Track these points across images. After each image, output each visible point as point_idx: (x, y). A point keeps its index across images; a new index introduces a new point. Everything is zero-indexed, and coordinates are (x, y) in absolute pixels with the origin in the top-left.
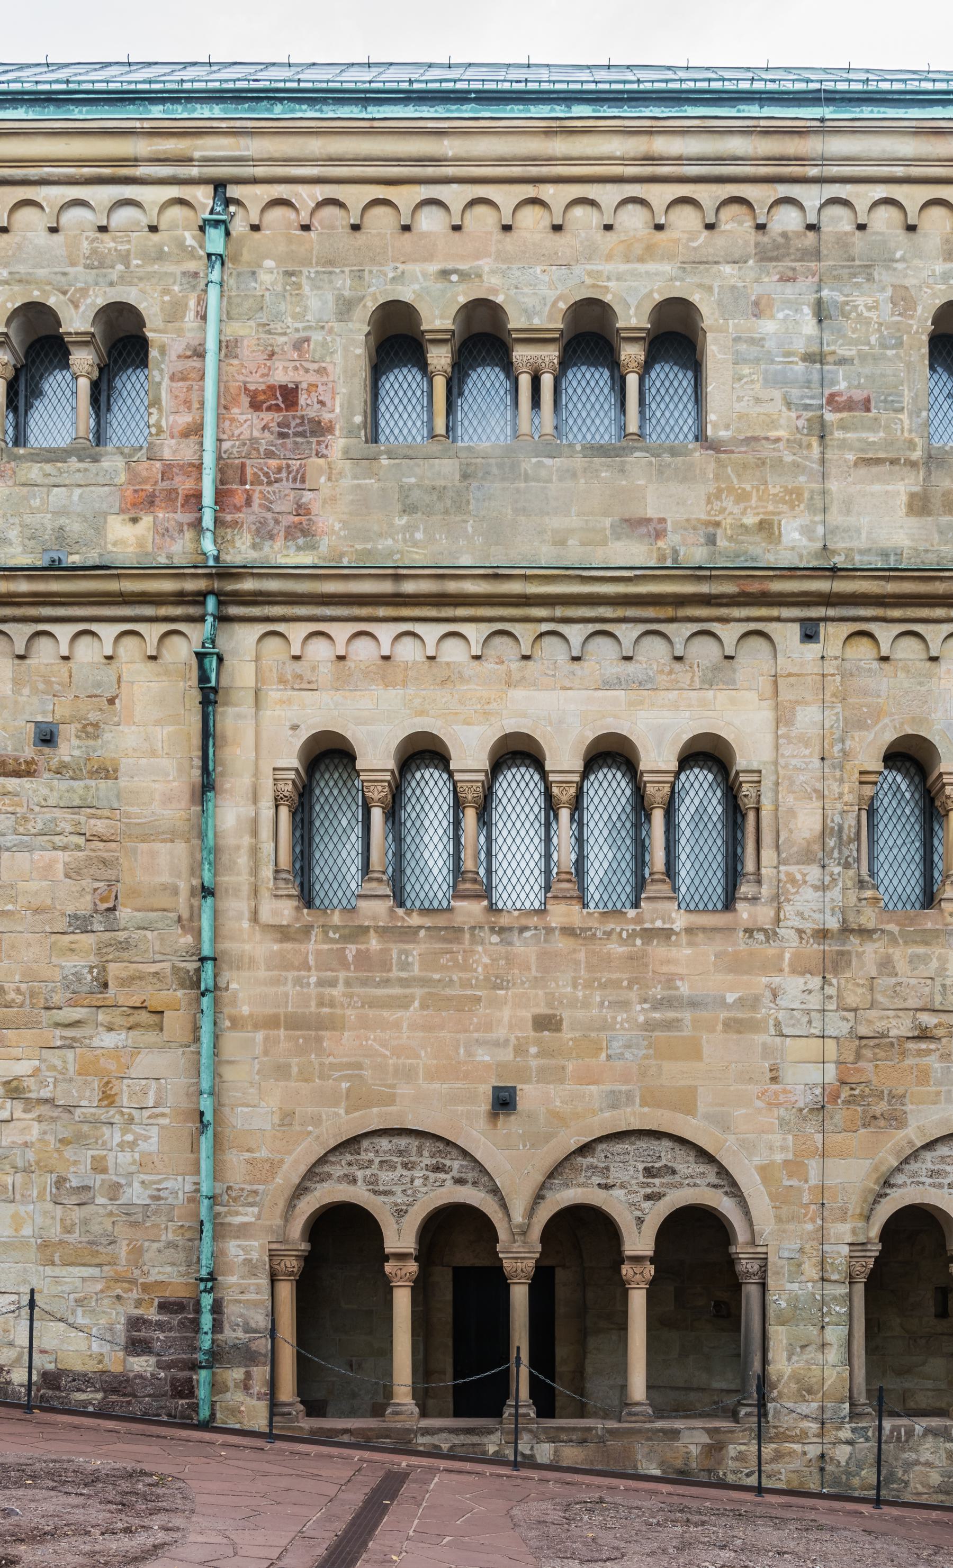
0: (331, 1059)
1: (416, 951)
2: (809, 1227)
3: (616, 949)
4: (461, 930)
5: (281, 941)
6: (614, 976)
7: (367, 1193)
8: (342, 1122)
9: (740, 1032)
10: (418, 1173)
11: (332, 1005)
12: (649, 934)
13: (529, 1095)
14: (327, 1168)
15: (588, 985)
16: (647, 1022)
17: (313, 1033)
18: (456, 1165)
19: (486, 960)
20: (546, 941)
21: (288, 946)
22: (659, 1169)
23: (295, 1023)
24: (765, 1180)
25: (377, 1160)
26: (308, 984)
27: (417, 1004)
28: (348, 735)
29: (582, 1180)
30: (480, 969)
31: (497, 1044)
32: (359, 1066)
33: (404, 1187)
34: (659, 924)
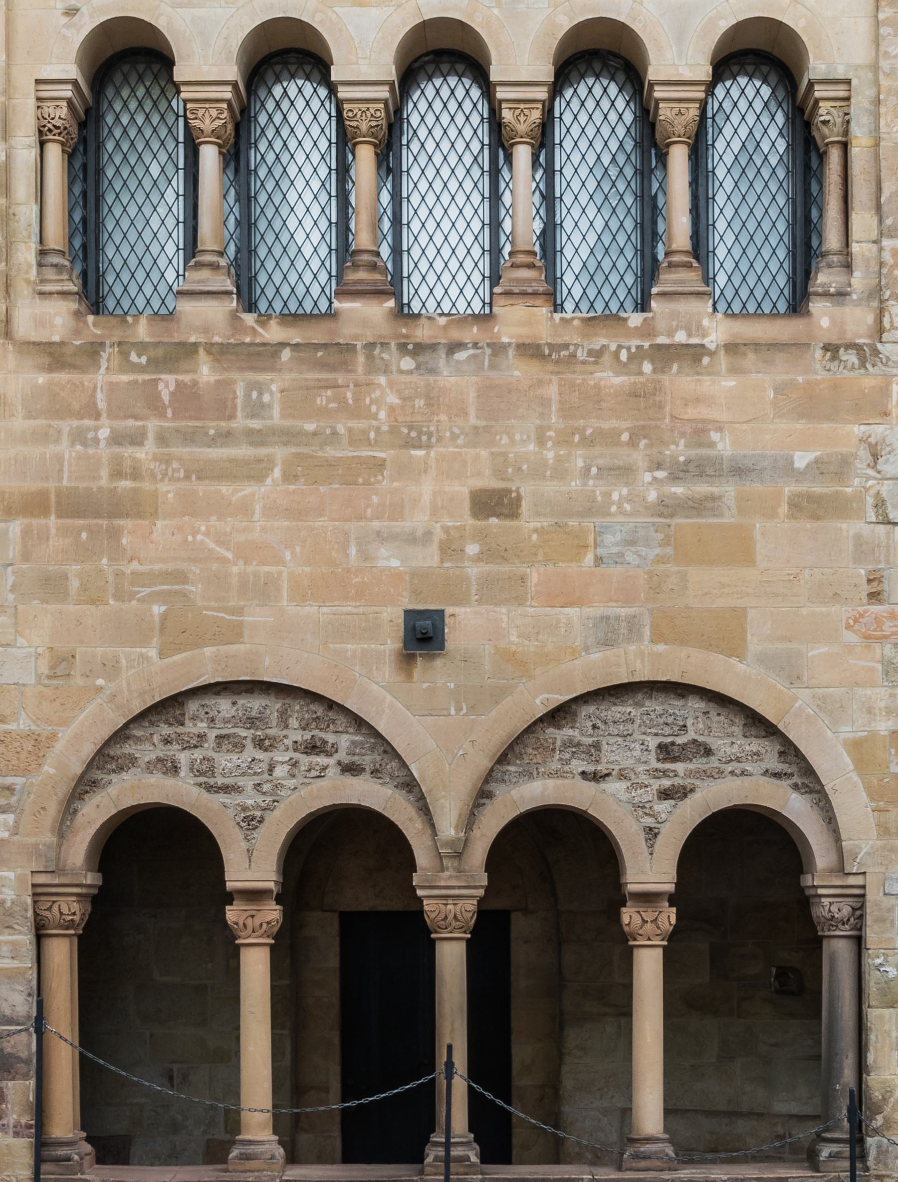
0: (135, 566)
1: (275, 385)
3: (611, 379)
4: (350, 348)
5: (50, 369)
6: (606, 425)
7: (195, 790)
8: (154, 671)
9: (817, 518)
10: (280, 756)
11: (136, 475)
12: (665, 355)
13: (465, 625)
14: (128, 748)
15: (564, 440)
16: (661, 502)
17: (104, 523)
18: (345, 741)
19: (393, 399)
20: (492, 367)
21: (63, 377)
22: (683, 747)
23: (74, 506)
24: (861, 764)
25: (212, 735)
26: (96, 441)
27: (277, 473)
28: (161, 24)
29: (555, 765)
30: (382, 415)
31: (411, 539)
32: (181, 577)
33: (257, 780)
34: (681, 337)
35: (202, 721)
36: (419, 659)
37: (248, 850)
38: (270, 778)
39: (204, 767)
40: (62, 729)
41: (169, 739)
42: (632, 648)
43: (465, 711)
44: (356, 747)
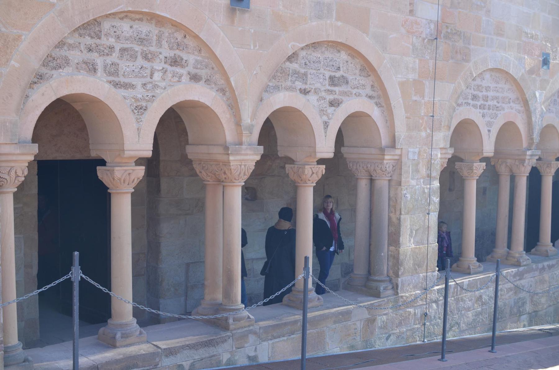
2: (423, 134)
7: (107, 85)
10: (158, 65)
22: (339, 78)
29: (289, 83)
33: (144, 81)
35: (112, 37)
36: (238, 12)
37: (138, 129)
38: (151, 80)
39: (112, 70)
40: (24, 32)
41: (91, 48)
42: (328, 22)
43: (258, 47)
44: (198, 64)
